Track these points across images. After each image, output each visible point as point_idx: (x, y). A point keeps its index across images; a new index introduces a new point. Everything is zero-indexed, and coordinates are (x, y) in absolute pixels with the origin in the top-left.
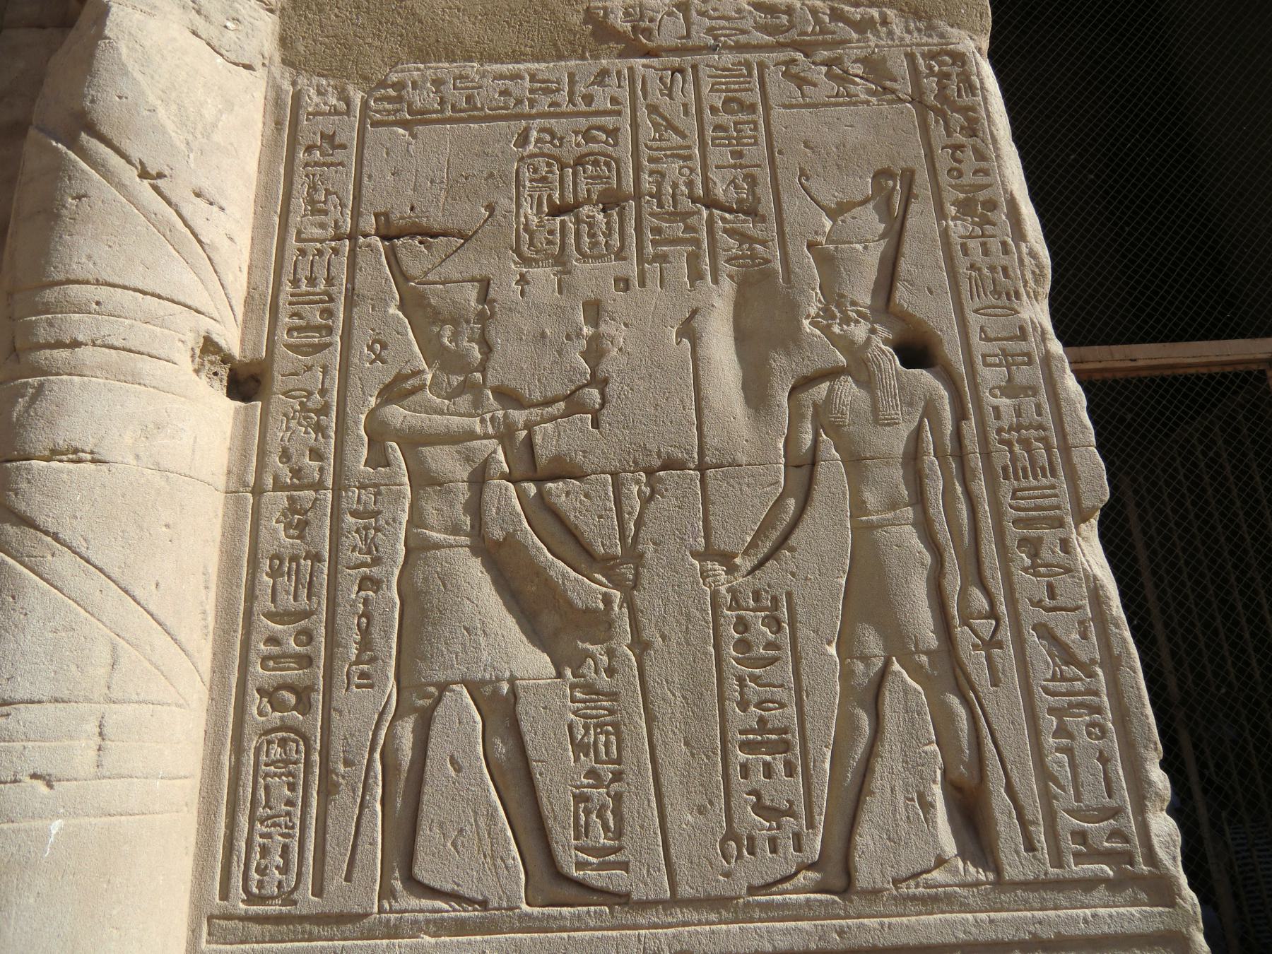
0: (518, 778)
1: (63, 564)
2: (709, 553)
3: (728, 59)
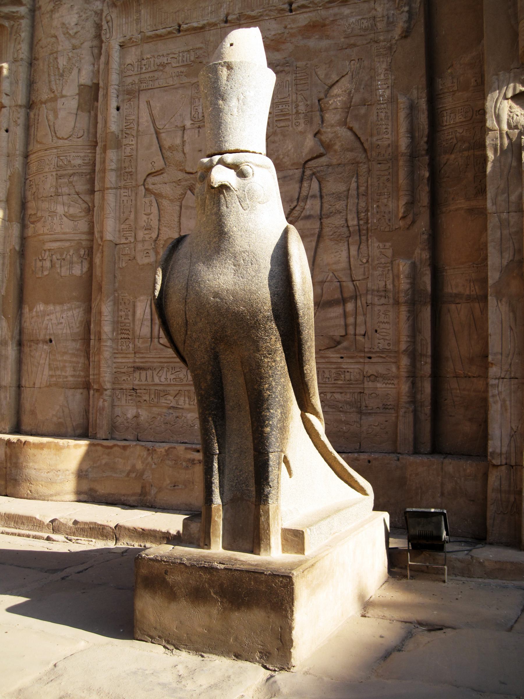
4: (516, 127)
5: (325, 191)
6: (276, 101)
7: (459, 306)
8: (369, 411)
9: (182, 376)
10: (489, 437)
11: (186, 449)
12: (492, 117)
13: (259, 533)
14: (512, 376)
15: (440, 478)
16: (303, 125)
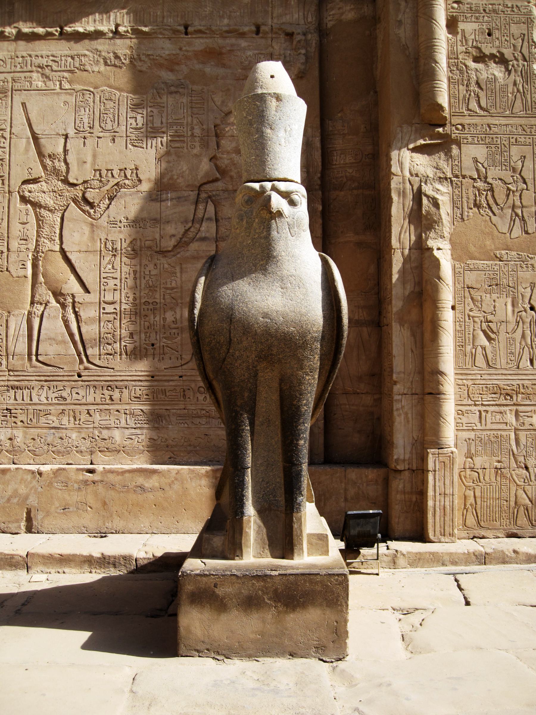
0: (486, 356)
1: (446, 332)
2: (507, 332)
3: (513, 263)
4: (417, 175)
5: (220, 214)
6: (170, 121)
9: (65, 394)
10: (395, 446)
11: (78, 470)
12: (396, 164)
13: (292, 539)
14: (414, 392)
15: (343, 485)
16: (199, 148)
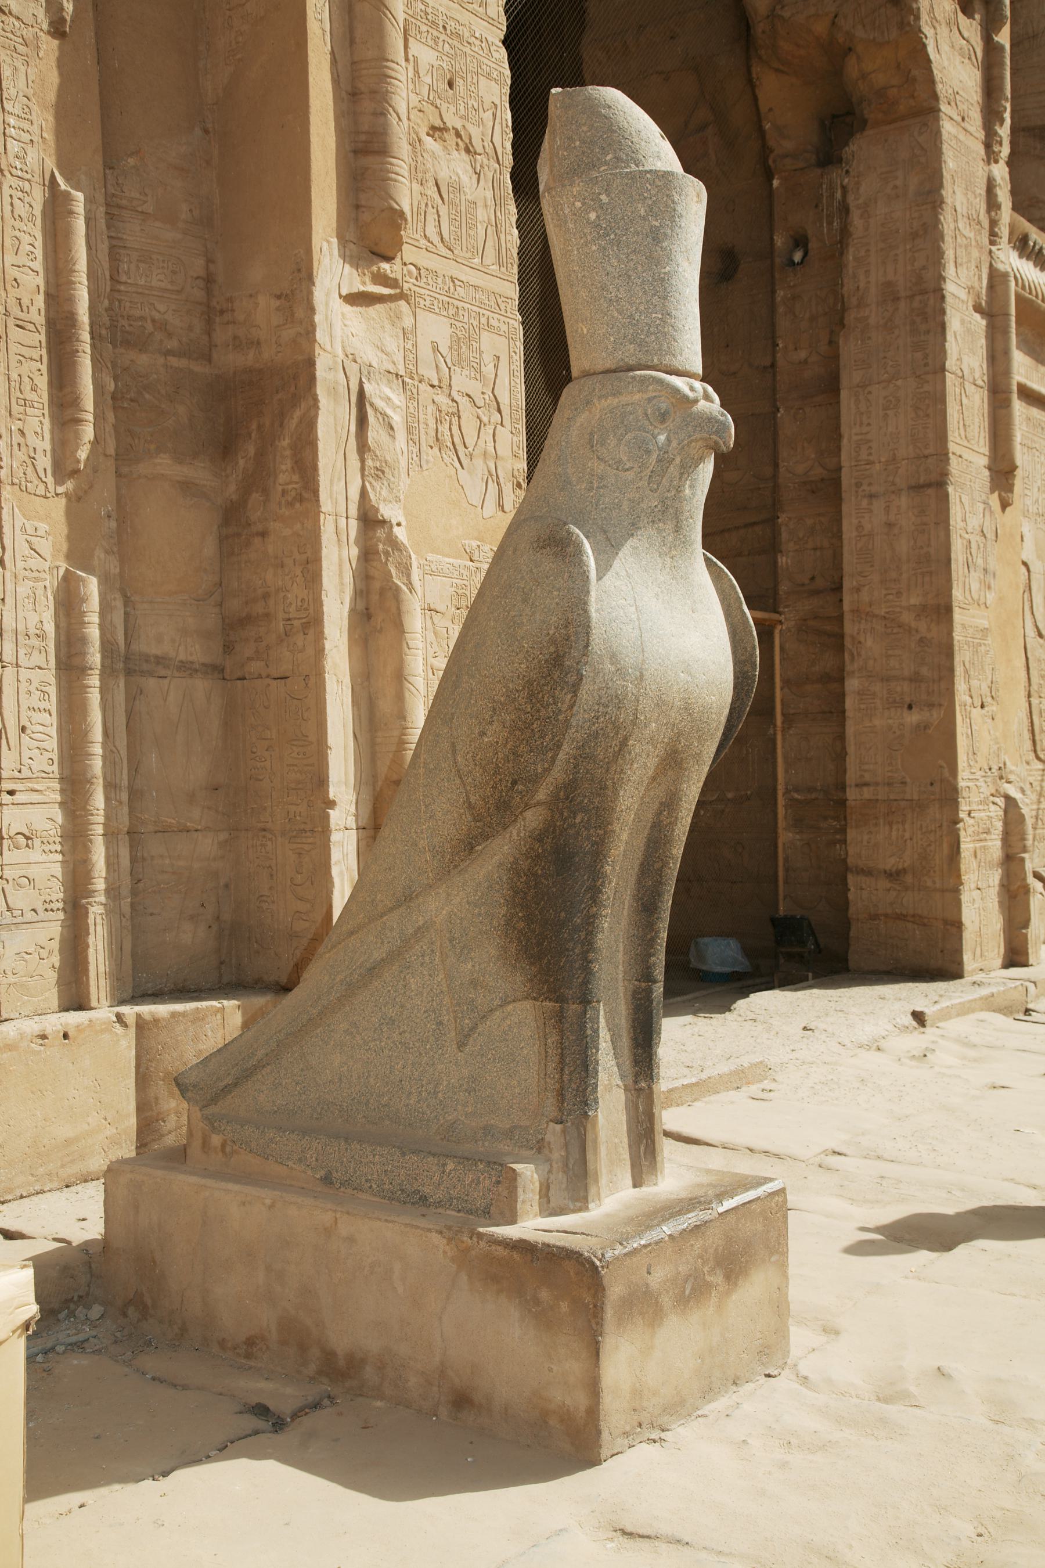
7: (166, 681)
8: (15, 921)
